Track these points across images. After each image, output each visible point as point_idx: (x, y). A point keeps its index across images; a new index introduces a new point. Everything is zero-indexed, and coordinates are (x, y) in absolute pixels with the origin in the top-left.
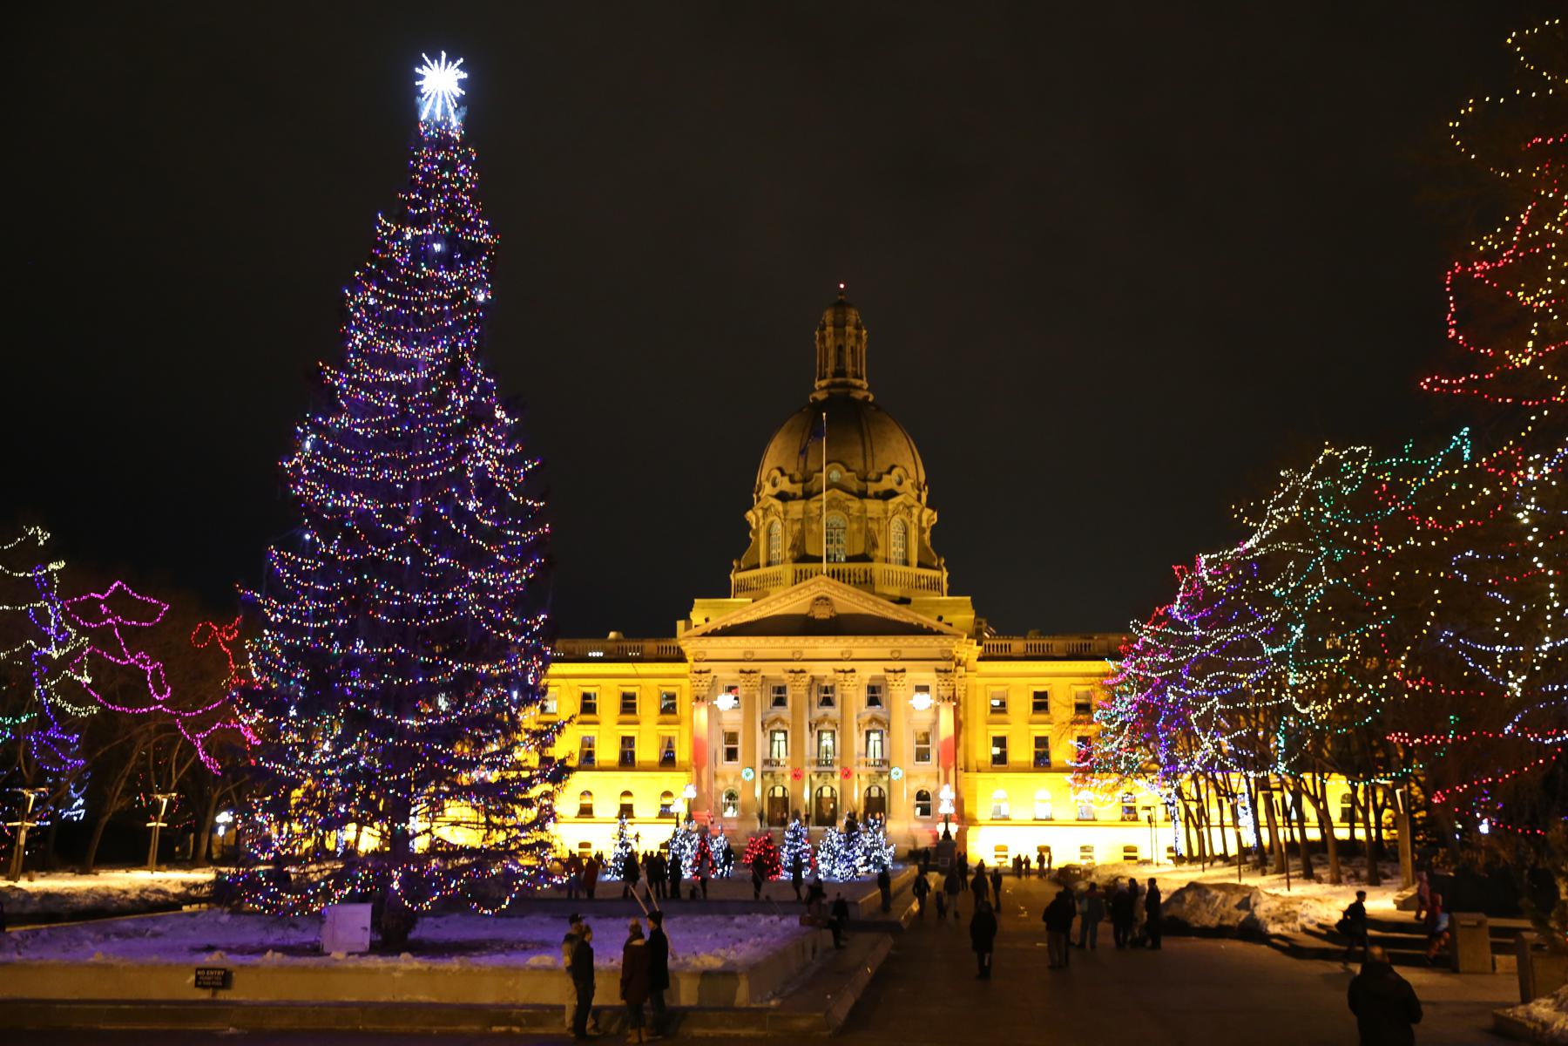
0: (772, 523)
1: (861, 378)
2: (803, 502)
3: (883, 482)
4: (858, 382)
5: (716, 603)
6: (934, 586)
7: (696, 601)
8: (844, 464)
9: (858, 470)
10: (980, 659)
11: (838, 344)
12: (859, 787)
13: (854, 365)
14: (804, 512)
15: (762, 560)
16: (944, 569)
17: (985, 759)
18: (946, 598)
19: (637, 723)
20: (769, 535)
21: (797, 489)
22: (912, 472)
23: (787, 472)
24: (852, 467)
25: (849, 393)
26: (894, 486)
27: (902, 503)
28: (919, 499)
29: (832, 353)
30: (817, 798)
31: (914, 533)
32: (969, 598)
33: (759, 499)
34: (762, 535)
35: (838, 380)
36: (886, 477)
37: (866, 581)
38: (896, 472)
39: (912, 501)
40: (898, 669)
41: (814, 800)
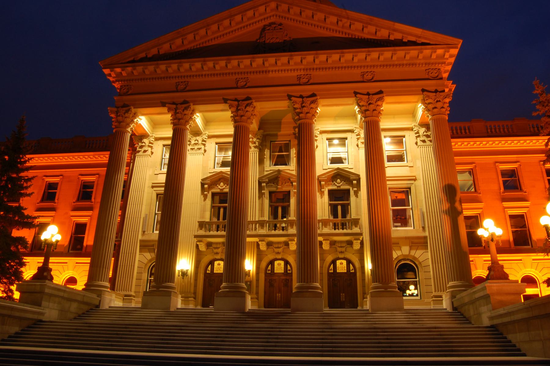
12: (323, 260)
40: (372, 91)
41: (262, 276)
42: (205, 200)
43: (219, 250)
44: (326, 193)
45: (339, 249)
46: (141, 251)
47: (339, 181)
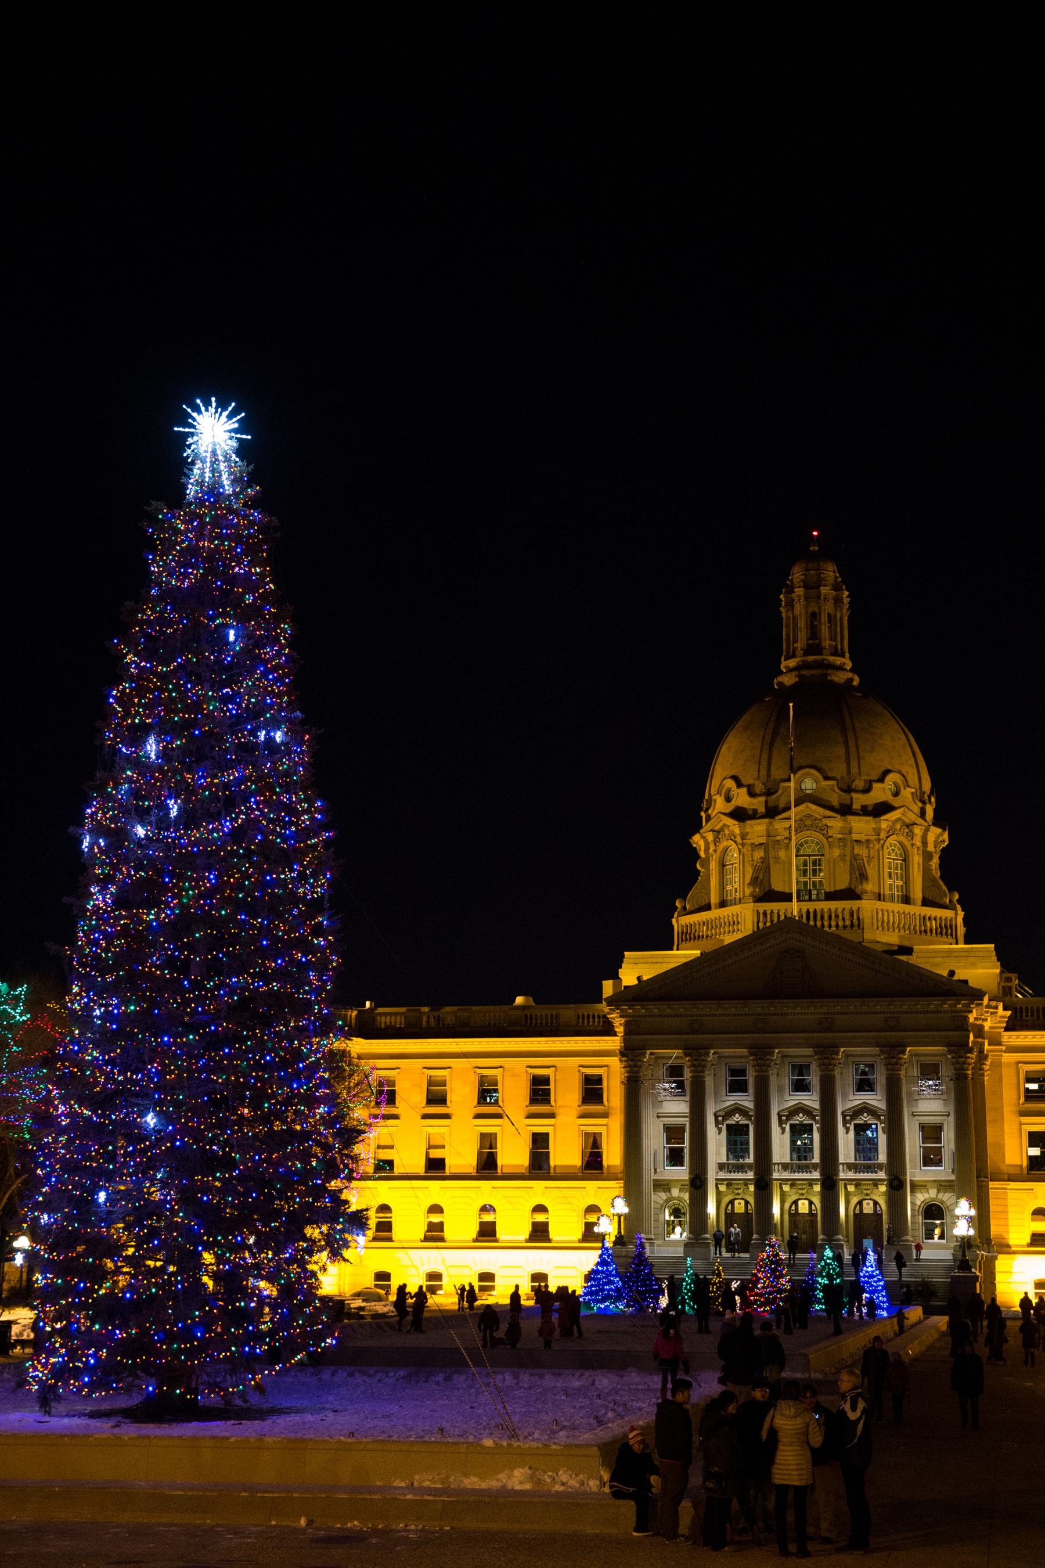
0: (726, 849)
1: (843, 655)
2: (766, 820)
3: (872, 794)
4: (838, 661)
5: (652, 957)
6: (946, 930)
7: (626, 953)
8: (819, 770)
9: (839, 777)
10: (1006, 1029)
11: (810, 610)
12: (847, 1202)
13: (833, 638)
14: (769, 836)
15: (714, 899)
16: (959, 907)
17: (1019, 1163)
18: (962, 946)
19: (552, 1116)
20: (723, 865)
21: (758, 804)
22: (913, 779)
23: (744, 782)
24: (830, 774)
25: (827, 675)
26: (888, 797)
27: (899, 819)
28: (923, 814)
29: (802, 624)
30: (790, 1214)
31: (916, 860)
32: (993, 946)
33: (708, 818)
34: (714, 865)
35: (811, 658)
36: (876, 786)
37: (852, 926)
38: (891, 778)
39: (912, 817)
41: (786, 1217)
42: (720, 1133)
43: (740, 1191)
44: (852, 1128)
45: (865, 1192)
46: (654, 1191)
47: (865, 1114)
